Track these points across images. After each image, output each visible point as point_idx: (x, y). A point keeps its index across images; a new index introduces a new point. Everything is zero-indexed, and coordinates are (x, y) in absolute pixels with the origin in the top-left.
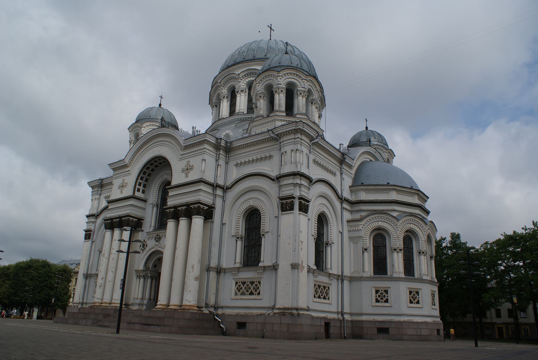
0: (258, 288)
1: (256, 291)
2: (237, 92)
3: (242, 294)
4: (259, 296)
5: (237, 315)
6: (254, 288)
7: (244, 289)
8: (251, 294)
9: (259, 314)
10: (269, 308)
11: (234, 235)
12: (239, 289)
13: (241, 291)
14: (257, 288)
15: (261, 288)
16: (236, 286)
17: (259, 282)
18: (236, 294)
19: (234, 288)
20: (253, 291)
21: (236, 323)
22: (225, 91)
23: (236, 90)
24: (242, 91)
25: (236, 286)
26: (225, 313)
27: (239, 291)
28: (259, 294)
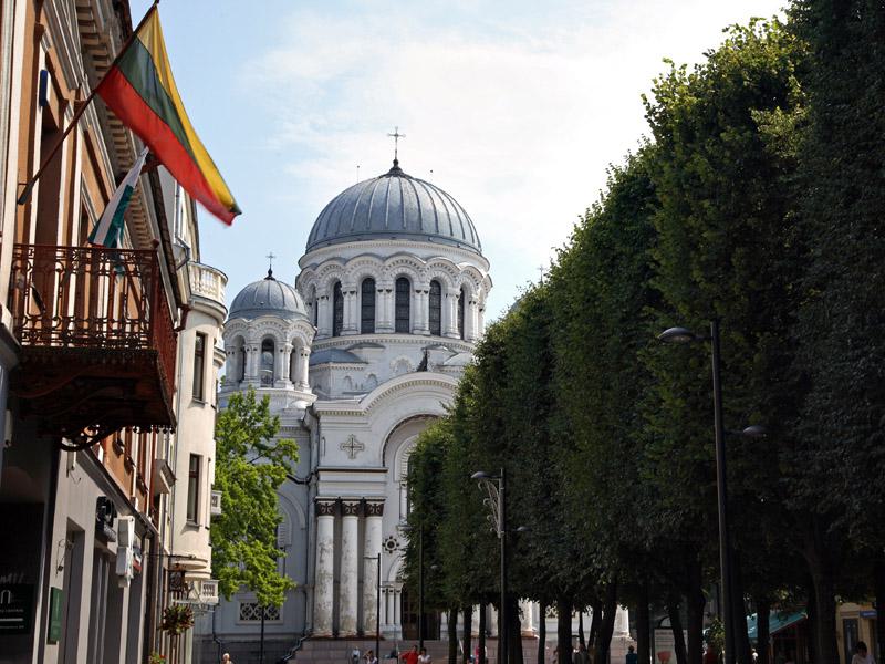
22: (324, 288)
24: (352, 293)
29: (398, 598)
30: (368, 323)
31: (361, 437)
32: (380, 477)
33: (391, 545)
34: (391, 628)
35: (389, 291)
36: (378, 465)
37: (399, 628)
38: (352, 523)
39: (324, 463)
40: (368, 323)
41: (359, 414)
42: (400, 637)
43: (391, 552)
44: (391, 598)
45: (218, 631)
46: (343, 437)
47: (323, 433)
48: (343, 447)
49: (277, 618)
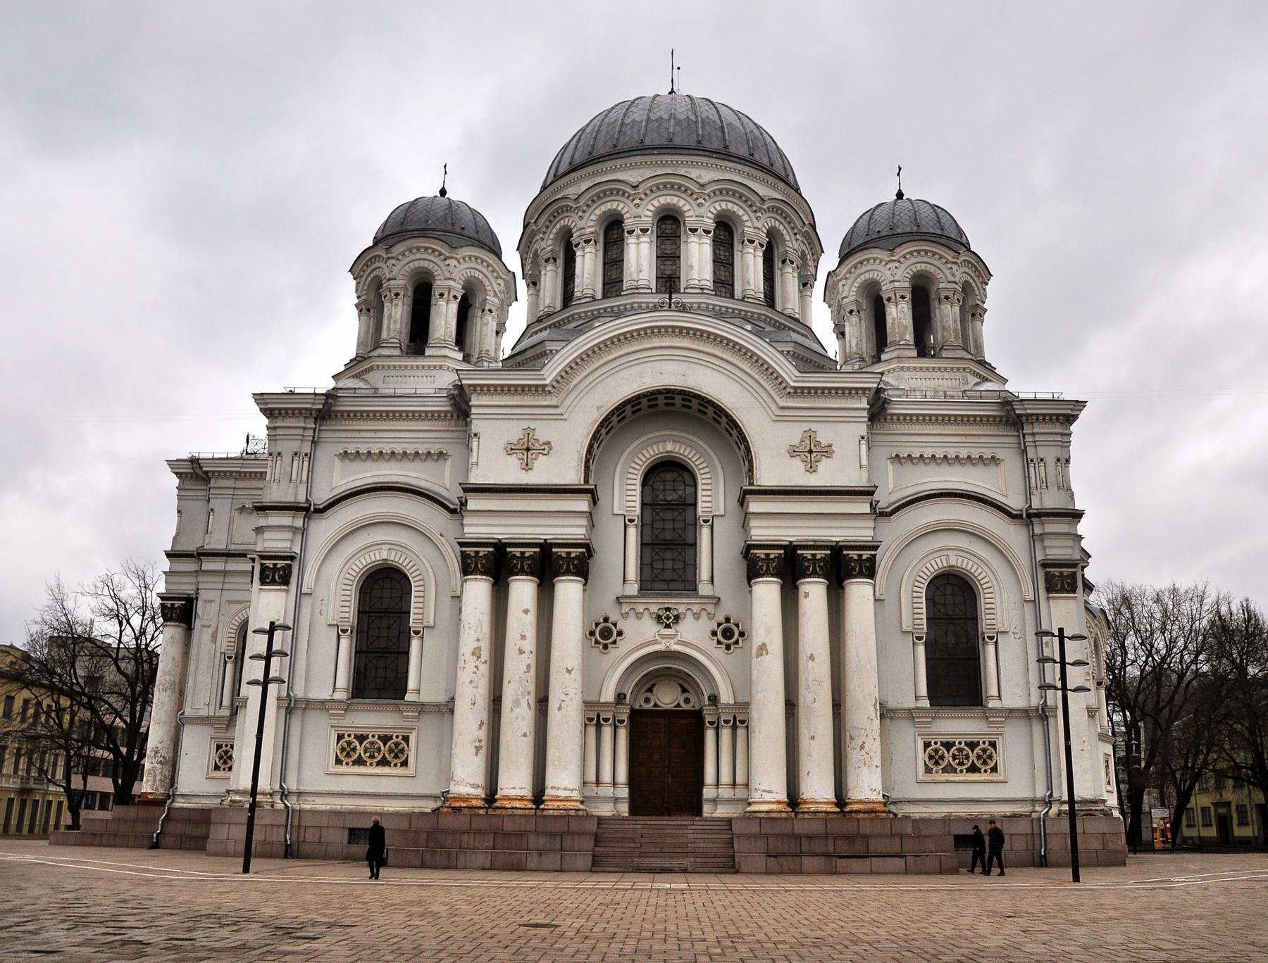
0: (990, 757)
1: (985, 763)
2: (577, 245)
3: (945, 770)
4: (995, 774)
5: (947, 820)
6: (979, 757)
7: (951, 759)
8: (973, 769)
9: (1008, 814)
10: (1033, 801)
11: (910, 629)
12: (935, 758)
13: (944, 764)
14: (986, 757)
15: (999, 758)
16: (927, 752)
17: (993, 745)
18: (928, 770)
19: (922, 756)
20: (979, 764)
21: (952, 838)
23: (574, 240)
25: (925, 752)
26: (911, 815)
27: (937, 763)
28: (994, 769)
29: (623, 734)
30: (613, 281)
31: (544, 432)
32: (582, 504)
33: (606, 633)
34: (607, 791)
35: (644, 231)
36: (572, 476)
37: (624, 792)
38: (523, 590)
39: (476, 478)
40: (613, 281)
41: (540, 390)
42: (624, 809)
43: (605, 647)
44: (607, 732)
45: (292, 785)
46: (513, 431)
47: (476, 426)
48: (511, 450)
49: (405, 764)
